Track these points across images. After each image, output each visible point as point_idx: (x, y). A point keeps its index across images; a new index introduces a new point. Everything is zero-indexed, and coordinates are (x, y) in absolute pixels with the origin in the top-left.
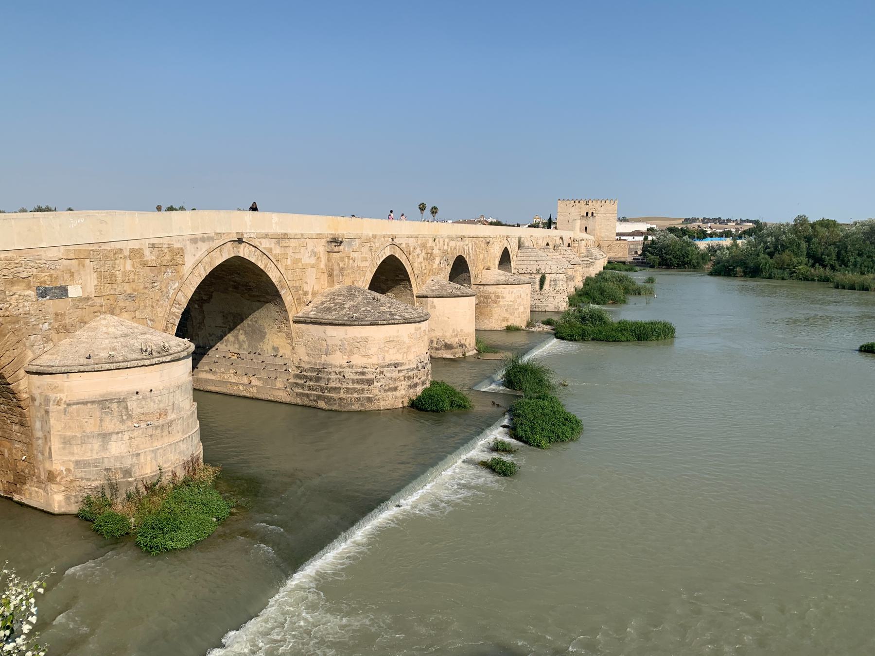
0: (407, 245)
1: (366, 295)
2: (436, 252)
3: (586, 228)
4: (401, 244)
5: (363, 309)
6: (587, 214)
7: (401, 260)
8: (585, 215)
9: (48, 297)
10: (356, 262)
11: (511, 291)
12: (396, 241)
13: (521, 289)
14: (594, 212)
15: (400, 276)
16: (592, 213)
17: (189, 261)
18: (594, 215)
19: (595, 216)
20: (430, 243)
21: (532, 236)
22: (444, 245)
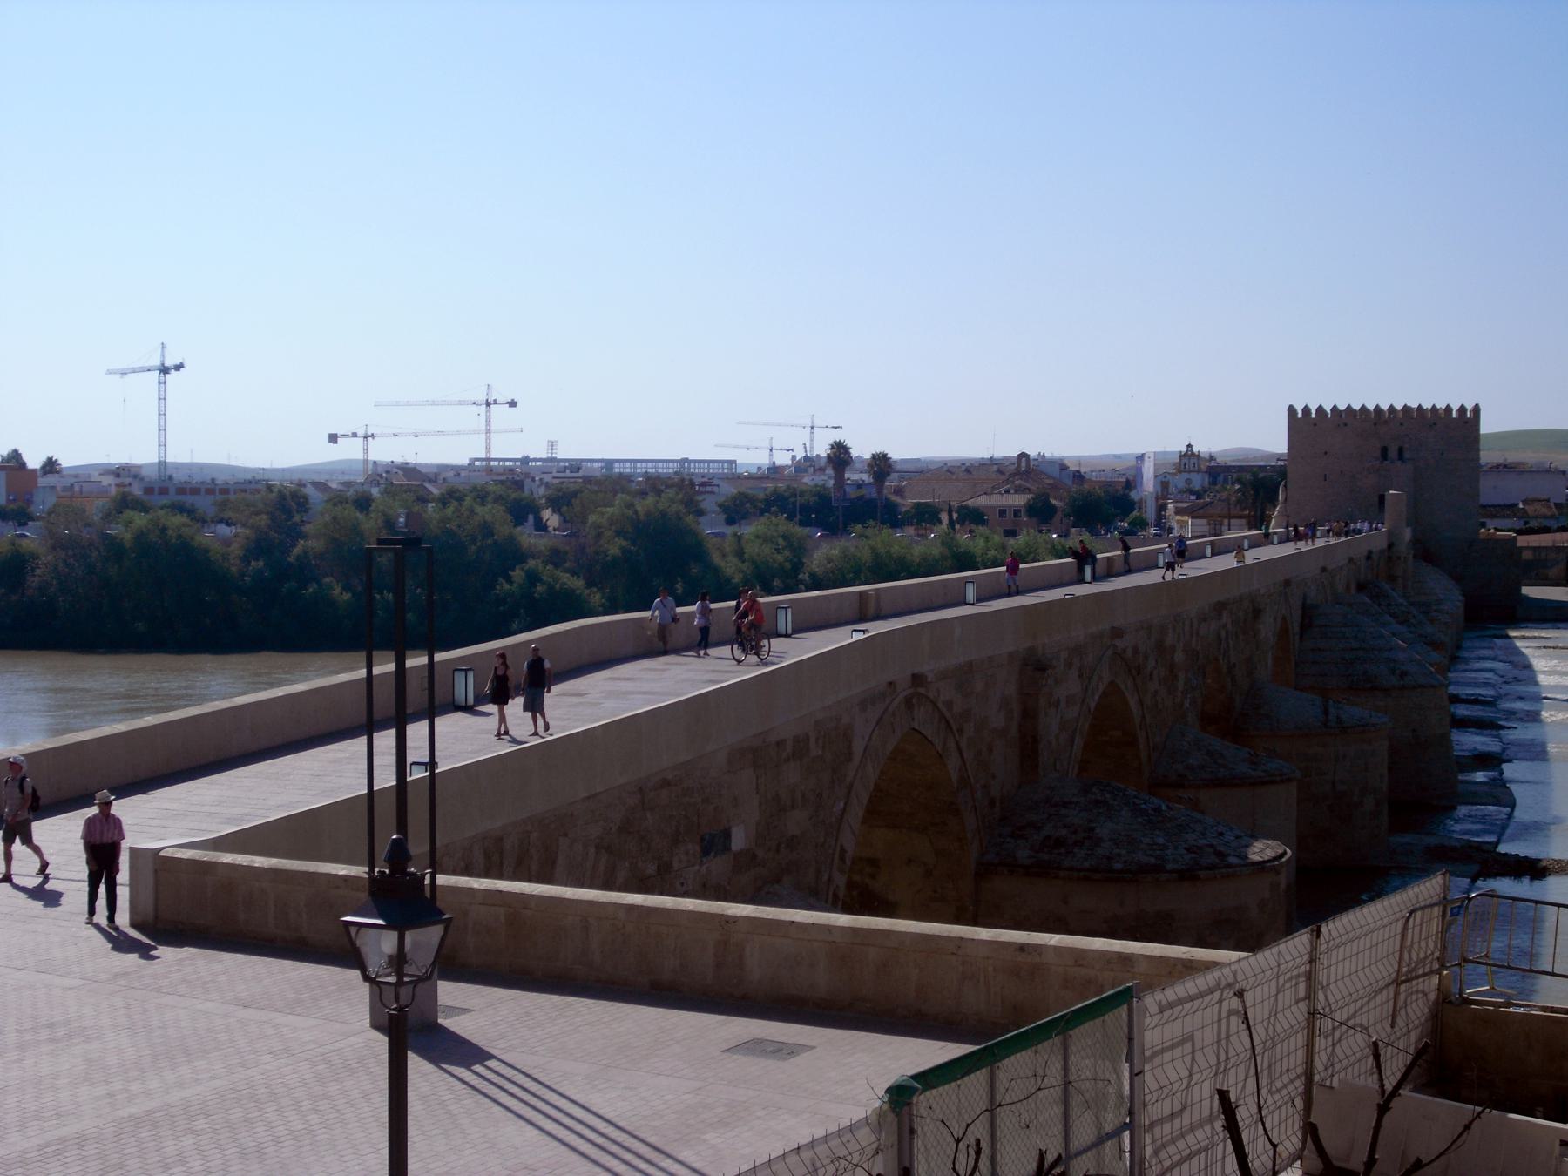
0: (1136, 650)
1: (1134, 803)
2: (1179, 656)
4: (1124, 651)
5: (1147, 840)
6: (1384, 451)
7: (1127, 694)
8: (1378, 453)
9: (712, 854)
12: (1119, 643)
14: (1407, 446)
16: (1401, 451)
17: (858, 747)
18: (1407, 455)
20: (1169, 640)
21: (1324, 570)
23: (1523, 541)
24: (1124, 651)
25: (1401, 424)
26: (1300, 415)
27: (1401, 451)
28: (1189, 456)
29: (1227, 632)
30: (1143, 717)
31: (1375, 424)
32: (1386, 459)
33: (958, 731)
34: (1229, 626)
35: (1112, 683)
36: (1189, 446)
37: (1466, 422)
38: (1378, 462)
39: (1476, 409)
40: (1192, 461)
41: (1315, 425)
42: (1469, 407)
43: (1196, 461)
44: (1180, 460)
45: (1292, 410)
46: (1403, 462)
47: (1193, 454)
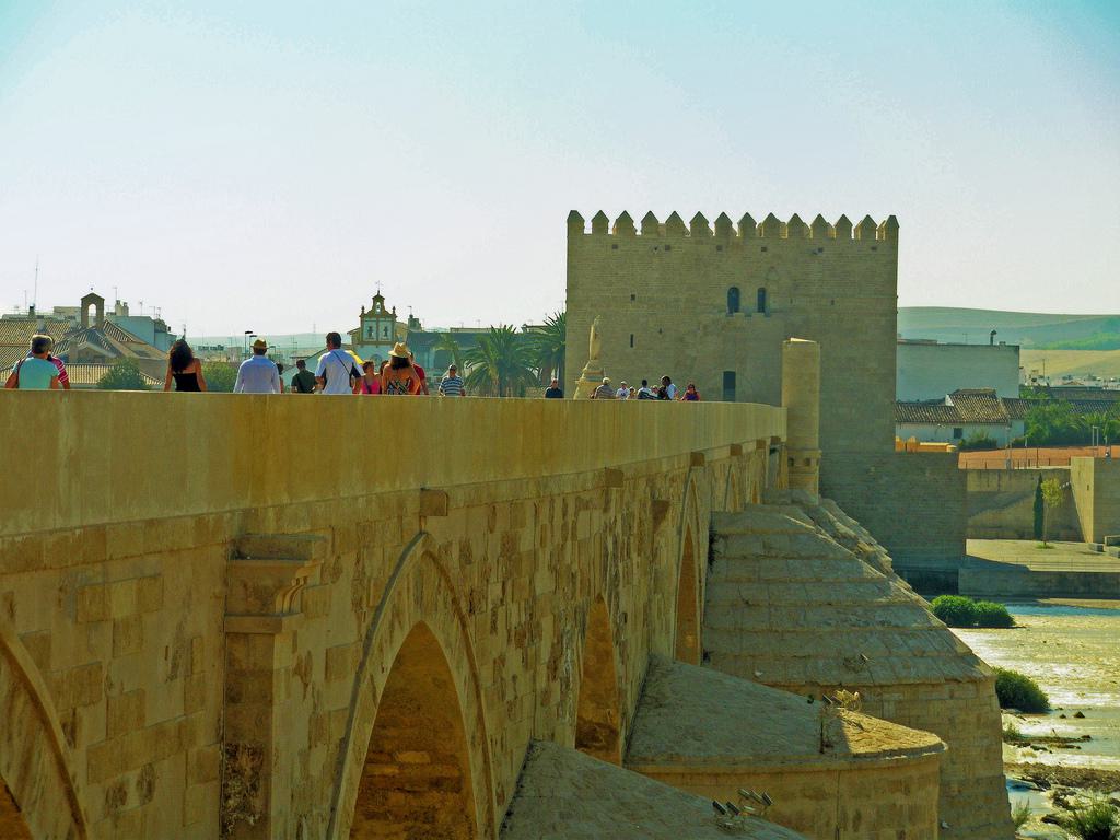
0: (466, 556)
3: (730, 379)
4: (447, 548)
6: (734, 296)
8: (723, 300)
10: (310, 686)
11: (851, 814)
13: (900, 799)
14: (771, 288)
15: (408, 757)
16: (762, 294)
18: (772, 303)
19: (775, 311)
22: (565, 539)
23: (968, 460)
24: (447, 548)
25: (764, 249)
26: (588, 229)
27: (762, 294)
28: (378, 316)
29: (615, 542)
30: (480, 718)
31: (719, 248)
32: (737, 311)
33: (64, 726)
34: (619, 529)
35: (421, 628)
36: (378, 299)
37: (874, 249)
38: (724, 314)
39: (892, 223)
40: (382, 325)
41: (615, 247)
42: (880, 219)
43: (389, 325)
44: (362, 322)
45: (574, 219)
46: (766, 316)
47: (384, 314)
